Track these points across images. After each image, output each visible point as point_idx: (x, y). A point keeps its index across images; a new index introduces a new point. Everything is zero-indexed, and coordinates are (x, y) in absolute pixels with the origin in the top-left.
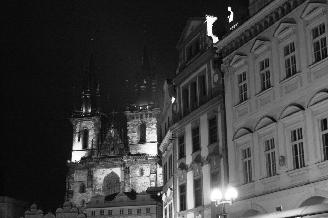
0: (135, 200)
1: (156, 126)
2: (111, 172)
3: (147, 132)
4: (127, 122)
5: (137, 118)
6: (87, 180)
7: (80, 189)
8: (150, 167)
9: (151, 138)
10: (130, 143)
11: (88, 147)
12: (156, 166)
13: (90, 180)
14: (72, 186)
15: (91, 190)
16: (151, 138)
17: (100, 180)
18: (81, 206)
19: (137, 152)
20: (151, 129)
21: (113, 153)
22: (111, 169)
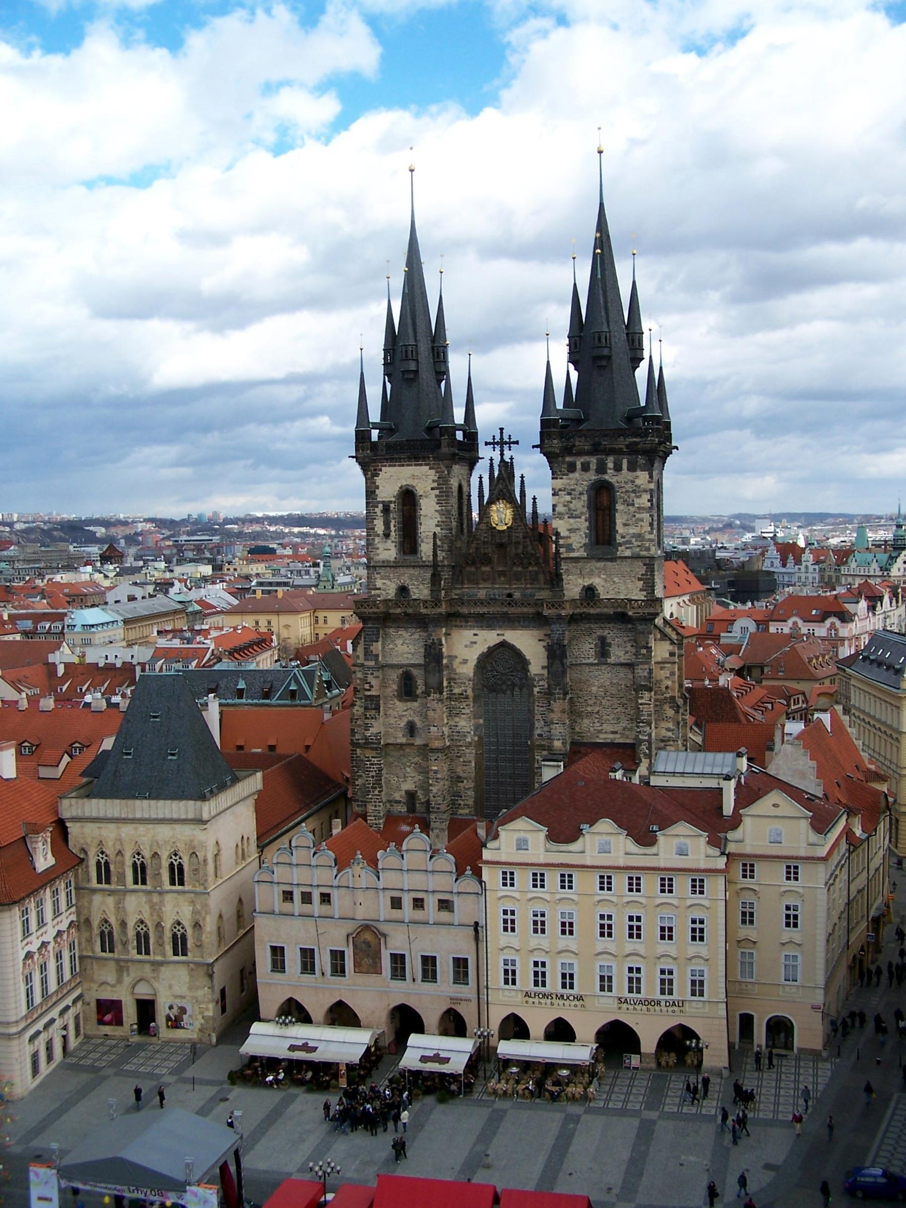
0: (653, 850)
1: (649, 501)
2: (498, 642)
3: (619, 520)
5: (585, 468)
6: (421, 661)
7: (400, 687)
14: (374, 682)
16: (634, 540)
17: (465, 666)
18: (404, 740)
19: (586, 584)
21: (503, 579)
22: (499, 632)
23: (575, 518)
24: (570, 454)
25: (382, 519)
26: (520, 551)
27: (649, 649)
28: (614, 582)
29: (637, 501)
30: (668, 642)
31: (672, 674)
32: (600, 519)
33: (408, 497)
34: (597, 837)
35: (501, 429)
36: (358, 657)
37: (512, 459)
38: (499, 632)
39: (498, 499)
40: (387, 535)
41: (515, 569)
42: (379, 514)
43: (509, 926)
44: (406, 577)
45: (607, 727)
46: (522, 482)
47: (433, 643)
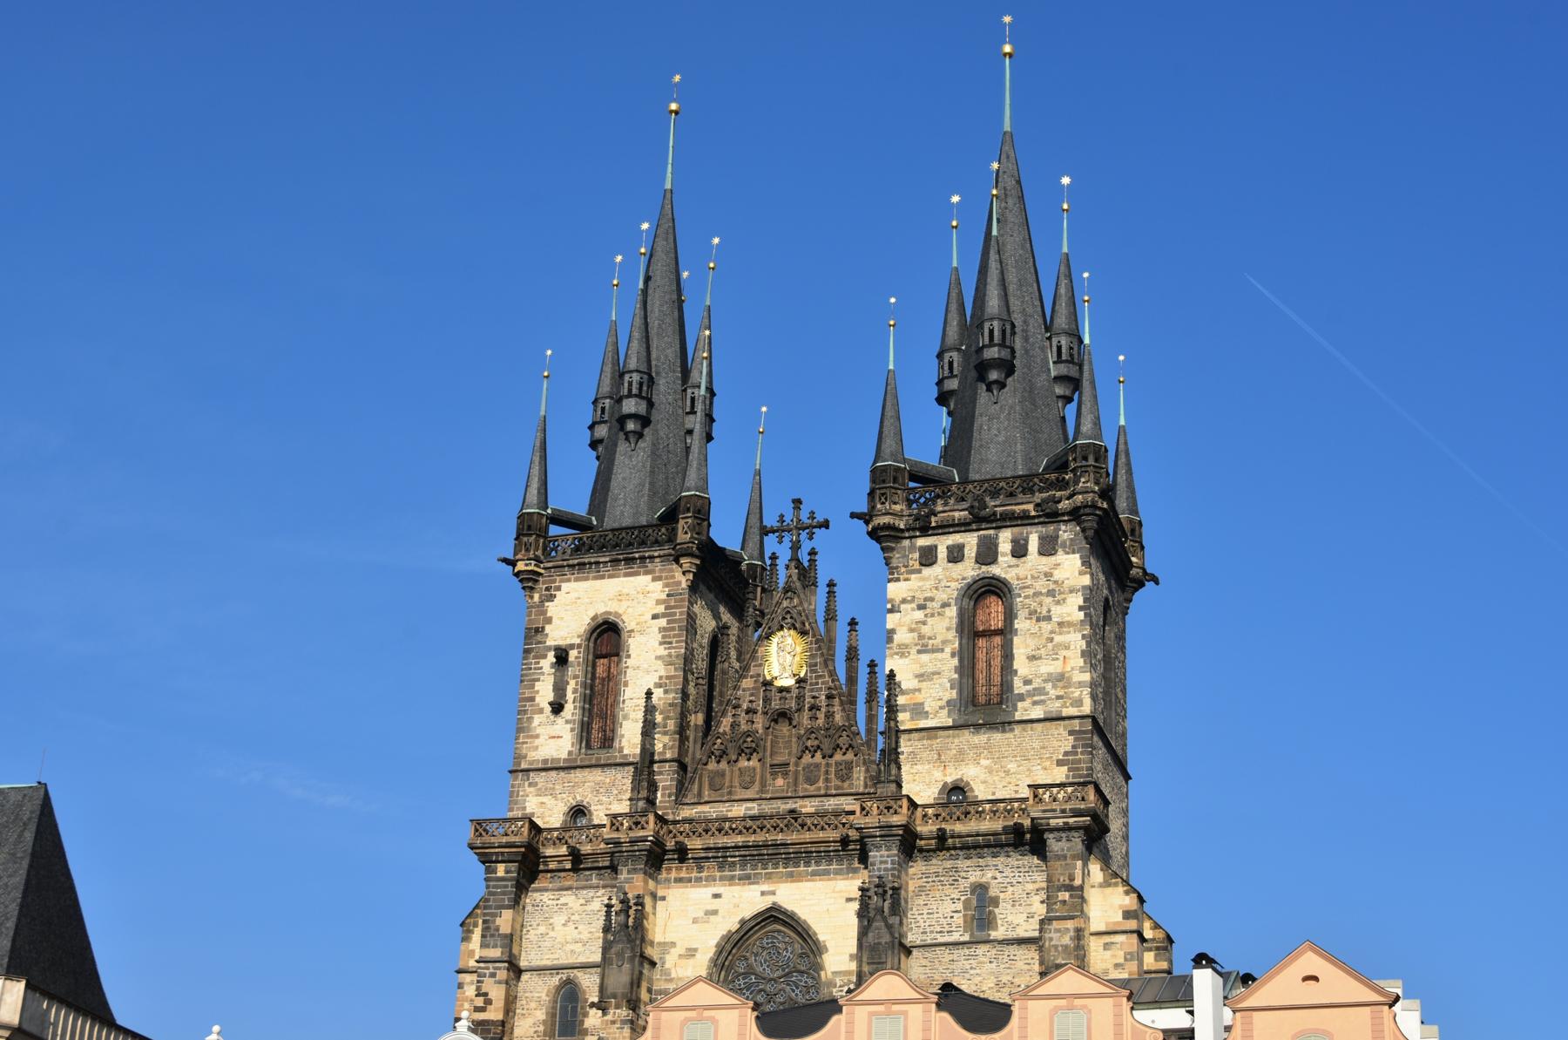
1: (1081, 608)
3: (1021, 648)
5: (956, 555)
8: (1040, 879)
9: (1049, 686)
10: (901, 716)
11: (616, 744)
12: (1086, 874)
13: (620, 955)
15: (623, 1022)
16: (1049, 686)
17: (691, 961)
19: (949, 780)
20: (1046, 627)
21: (780, 782)
22: (765, 887)
23: (933, 651)
24: (925, 530)
25: (552, 679)
26: (821, 721)
27: (1078, 892)
28: (1007, 772)
29: (1058, 612)
30: (1121, 889)
31: (1128, 957)
32: (981, 655)
33: (607, 636)
35: (797, 503)
37: (813, 553)
38: (765, 887)
39: (782, 628)
40: (557, 708)
41: (807, 759)
46: (831, 594)
47: (625, 902)
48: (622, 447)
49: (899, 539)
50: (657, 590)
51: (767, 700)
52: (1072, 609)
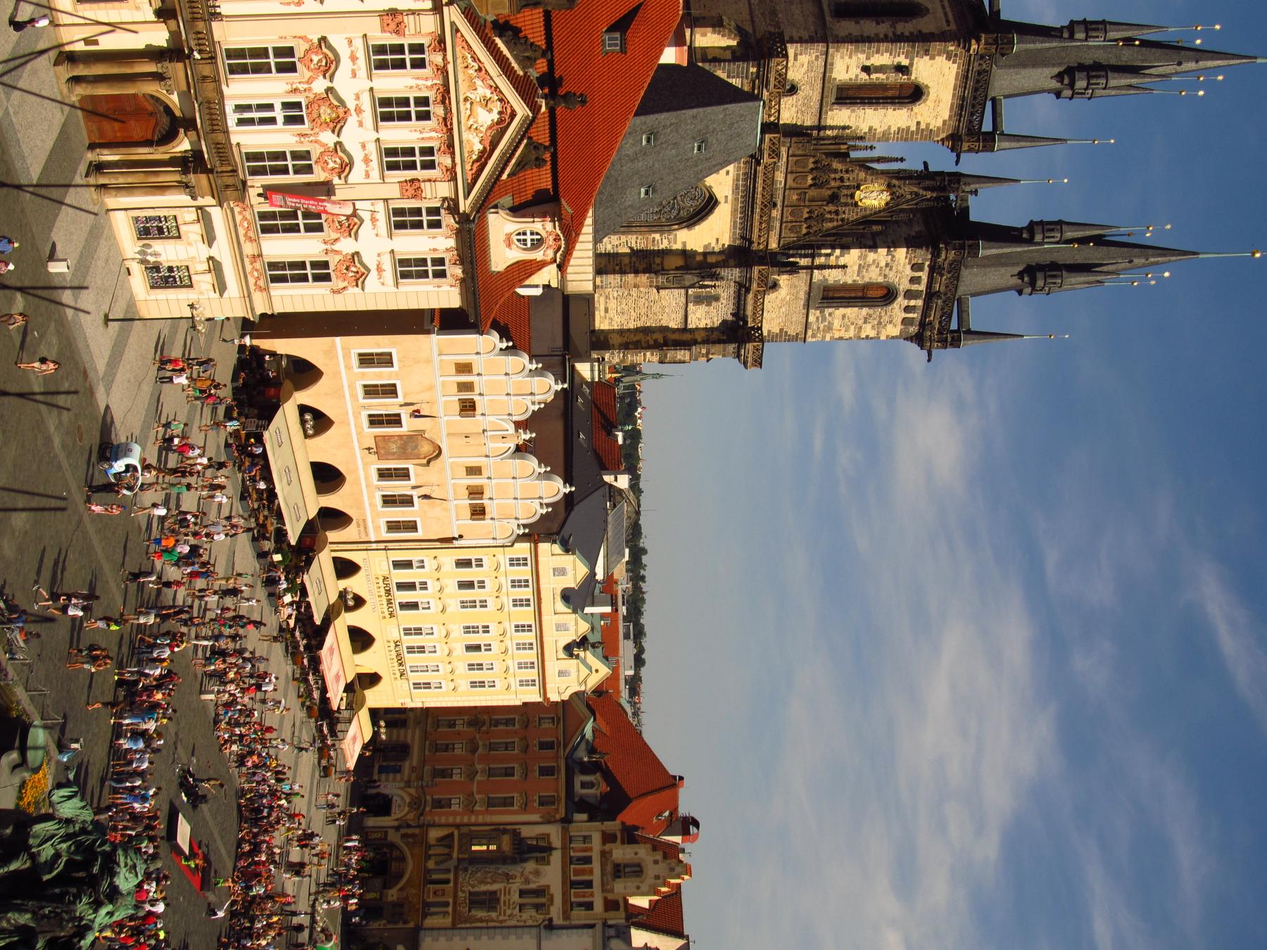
3: (851, 312)
4: (908, 248)
5: (913, 280)
20: (860, 322)
21: (795, 197)
22: (730, 198)
24: (932, 269)
25: (889, 63)
26: (828, 216)
29: (869, 326)
34: (573, 623)
36: (704, 35)
40: (866, 69)
41: (807, 210)
42: (897, 60)
43: (464, 564)
44: (810, 92)
45: (612, 304)
48: (1056, 70)
49: (932, 254)
50: (936, 123)
51: (848, 187)
52: (868, 331)
